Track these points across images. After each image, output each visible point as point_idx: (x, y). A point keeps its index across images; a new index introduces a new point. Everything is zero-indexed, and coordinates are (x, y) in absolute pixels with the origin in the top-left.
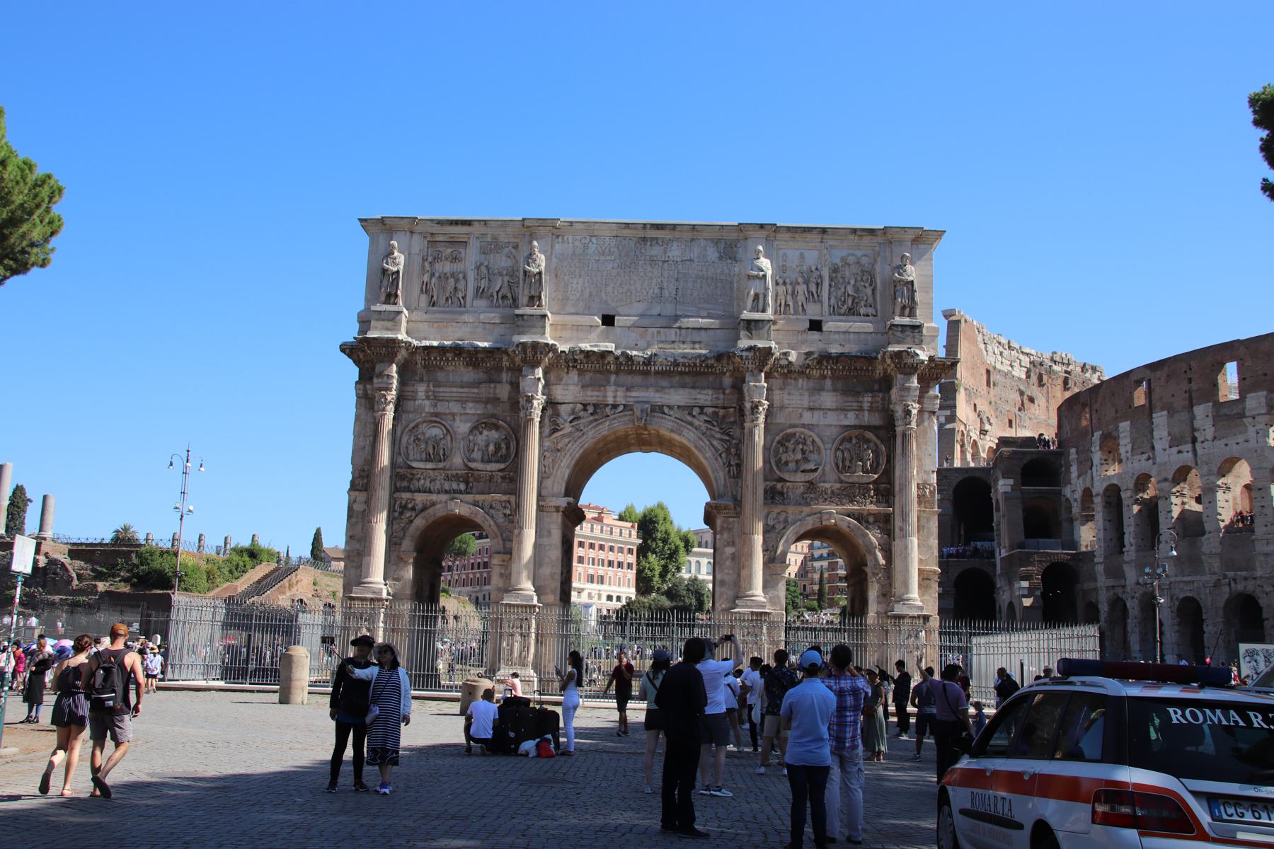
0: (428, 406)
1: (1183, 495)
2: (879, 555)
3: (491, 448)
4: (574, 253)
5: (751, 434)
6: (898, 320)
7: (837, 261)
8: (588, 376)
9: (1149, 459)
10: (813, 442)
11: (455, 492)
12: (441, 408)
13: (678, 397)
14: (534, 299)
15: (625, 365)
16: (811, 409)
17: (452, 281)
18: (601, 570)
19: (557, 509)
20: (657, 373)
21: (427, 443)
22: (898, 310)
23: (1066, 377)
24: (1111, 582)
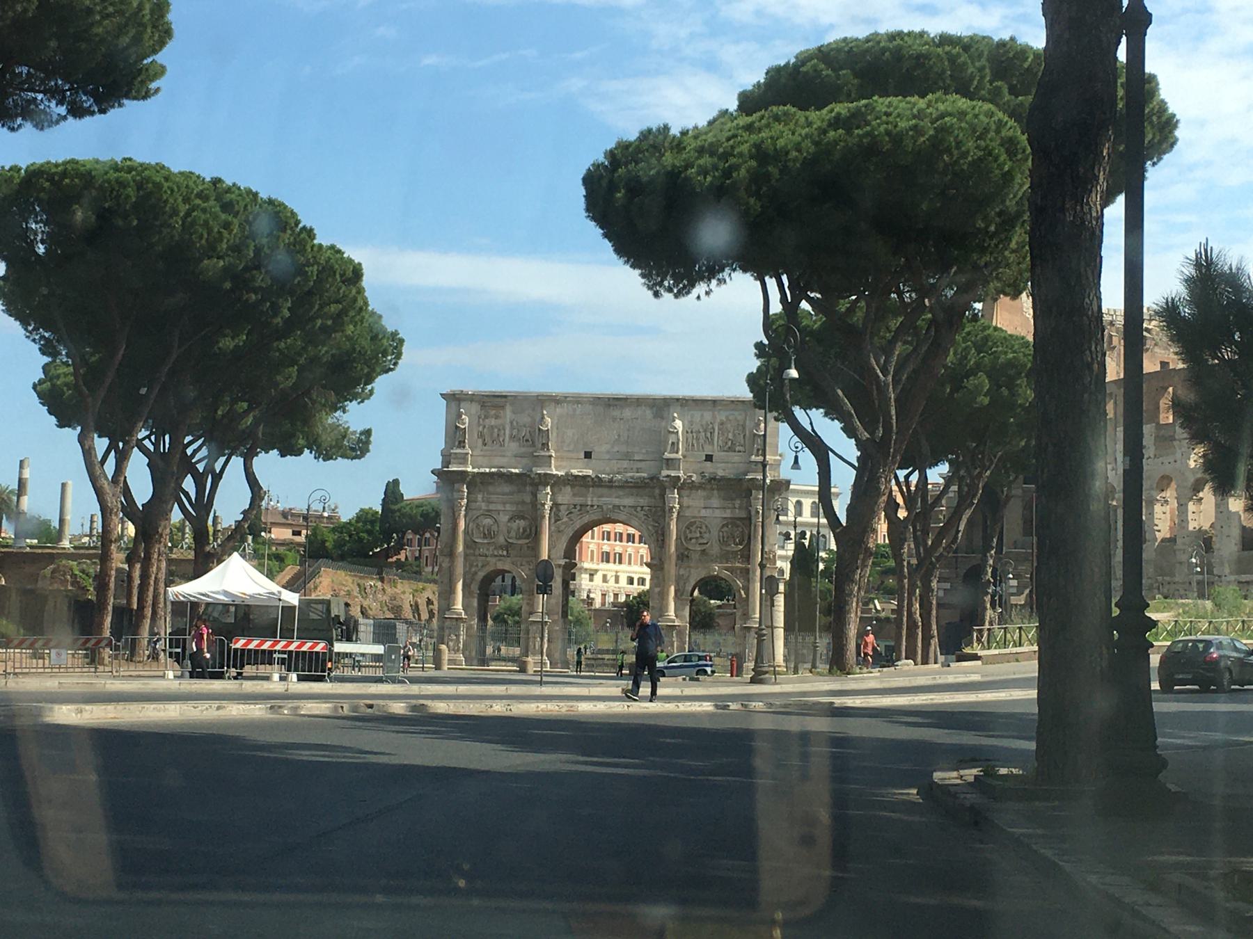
0: (484, 506)
2: (742, 592)
3: (521, 530)
4: (567, 414)
6: (753, 458)
7: (724, 419)
8: (577, 488)
9: (1113, 469)
11: (501, 556)
12: (492, 507)
13: (629, 501)
14: (545, 446)
15: (597, 483)
16: (705, 508)
17: (496, 430)
18: (618, 547)
22: (755, 451)
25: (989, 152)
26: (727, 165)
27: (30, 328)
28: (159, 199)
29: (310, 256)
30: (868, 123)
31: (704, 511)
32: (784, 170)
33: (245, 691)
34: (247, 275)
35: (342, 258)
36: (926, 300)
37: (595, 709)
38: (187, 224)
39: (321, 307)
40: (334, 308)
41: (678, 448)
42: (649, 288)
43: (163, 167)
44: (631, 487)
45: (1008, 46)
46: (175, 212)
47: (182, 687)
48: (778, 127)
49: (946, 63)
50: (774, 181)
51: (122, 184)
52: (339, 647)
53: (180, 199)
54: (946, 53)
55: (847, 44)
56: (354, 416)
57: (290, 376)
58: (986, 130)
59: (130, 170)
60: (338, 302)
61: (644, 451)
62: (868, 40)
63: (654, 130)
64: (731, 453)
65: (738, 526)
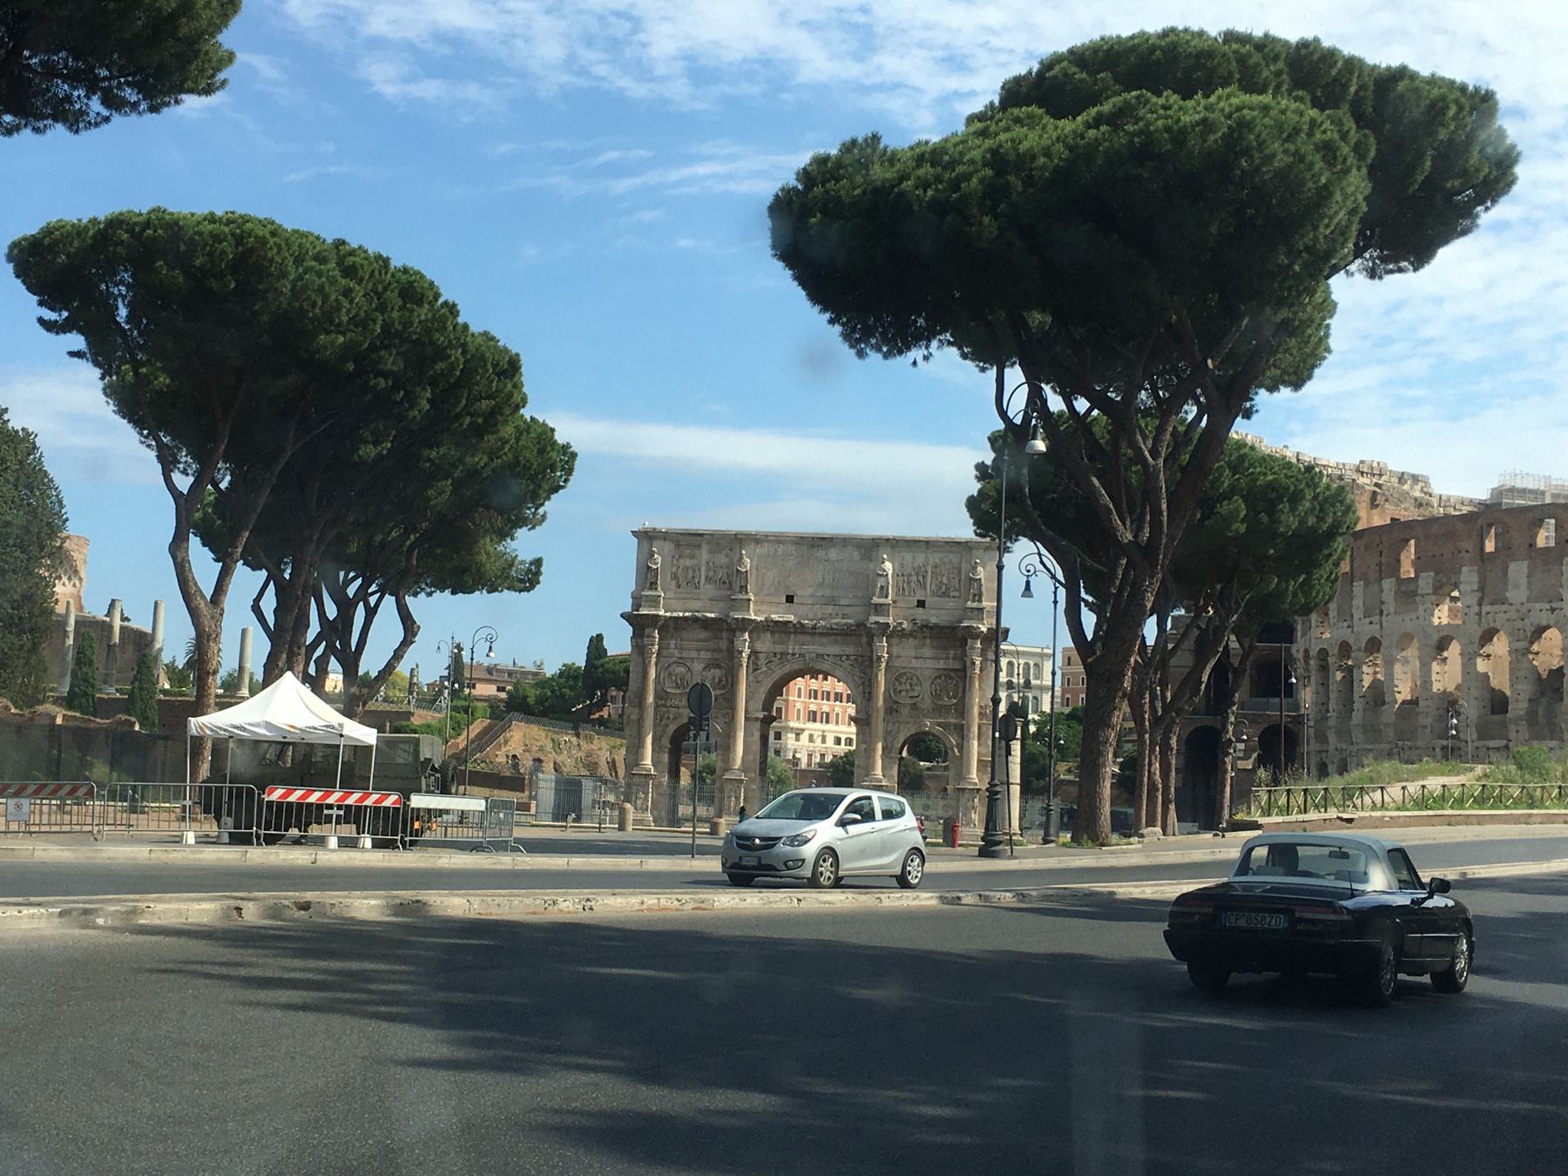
1: (1376, 665)
2: (956, 750)
3: (717, 680)
5: (877, 675)
8: (777, 635)
9: (1349, 627)
10: (918, 678)
12: (685, 654)
13: (834, 650)
14: (743, 589)
15: (798, 629)
16: (916, 658)
17: (690, 571)
19: (757, 719)
20: (820, 633)
21: (676, 676)
22: (971, 597)
23: (1374, 492)
24: (1318, 747)
25: (1300, 157)
26: (953, 174)
27: (145, 432)
28: (264, 258)
29: (452, 336)
30: (1137, 120)
31: (914, 661)
32: (1029, 181)
33: (249, 863)
34: (374, 356)
35: (496, 347)
36: (1209, 361)
37: (742, 905)
38: (298, 288)
39: (473, 400)
40: (485, 405)
41: (888, 593)
42: (852, 346)
43: (273, 223)
44: (835, 634)
45: (1311, 48)
46: (284, 275)
47: (153, 855)
48: (1019, 131)
49: (1234, 63)
50: (1014, 195)
51: (217, 238)
52: (418, 801)
53: (292, 259)
54: (1234, 52)
55: (1106, 43)
56: (523, 545)
57: (444, 492)
58: (1297, 131)
59: (229, 222)
60: (489, 397)
61: (851, 595)
62: (1132, 38)
63: (860, 140)
64: (947, 599)
65: (952, 678)
